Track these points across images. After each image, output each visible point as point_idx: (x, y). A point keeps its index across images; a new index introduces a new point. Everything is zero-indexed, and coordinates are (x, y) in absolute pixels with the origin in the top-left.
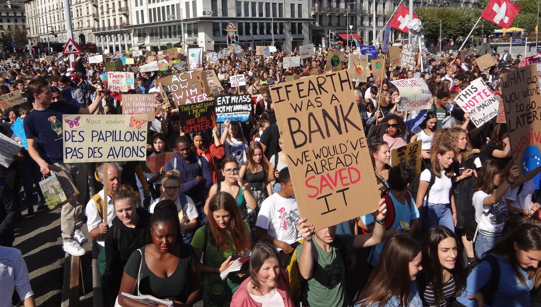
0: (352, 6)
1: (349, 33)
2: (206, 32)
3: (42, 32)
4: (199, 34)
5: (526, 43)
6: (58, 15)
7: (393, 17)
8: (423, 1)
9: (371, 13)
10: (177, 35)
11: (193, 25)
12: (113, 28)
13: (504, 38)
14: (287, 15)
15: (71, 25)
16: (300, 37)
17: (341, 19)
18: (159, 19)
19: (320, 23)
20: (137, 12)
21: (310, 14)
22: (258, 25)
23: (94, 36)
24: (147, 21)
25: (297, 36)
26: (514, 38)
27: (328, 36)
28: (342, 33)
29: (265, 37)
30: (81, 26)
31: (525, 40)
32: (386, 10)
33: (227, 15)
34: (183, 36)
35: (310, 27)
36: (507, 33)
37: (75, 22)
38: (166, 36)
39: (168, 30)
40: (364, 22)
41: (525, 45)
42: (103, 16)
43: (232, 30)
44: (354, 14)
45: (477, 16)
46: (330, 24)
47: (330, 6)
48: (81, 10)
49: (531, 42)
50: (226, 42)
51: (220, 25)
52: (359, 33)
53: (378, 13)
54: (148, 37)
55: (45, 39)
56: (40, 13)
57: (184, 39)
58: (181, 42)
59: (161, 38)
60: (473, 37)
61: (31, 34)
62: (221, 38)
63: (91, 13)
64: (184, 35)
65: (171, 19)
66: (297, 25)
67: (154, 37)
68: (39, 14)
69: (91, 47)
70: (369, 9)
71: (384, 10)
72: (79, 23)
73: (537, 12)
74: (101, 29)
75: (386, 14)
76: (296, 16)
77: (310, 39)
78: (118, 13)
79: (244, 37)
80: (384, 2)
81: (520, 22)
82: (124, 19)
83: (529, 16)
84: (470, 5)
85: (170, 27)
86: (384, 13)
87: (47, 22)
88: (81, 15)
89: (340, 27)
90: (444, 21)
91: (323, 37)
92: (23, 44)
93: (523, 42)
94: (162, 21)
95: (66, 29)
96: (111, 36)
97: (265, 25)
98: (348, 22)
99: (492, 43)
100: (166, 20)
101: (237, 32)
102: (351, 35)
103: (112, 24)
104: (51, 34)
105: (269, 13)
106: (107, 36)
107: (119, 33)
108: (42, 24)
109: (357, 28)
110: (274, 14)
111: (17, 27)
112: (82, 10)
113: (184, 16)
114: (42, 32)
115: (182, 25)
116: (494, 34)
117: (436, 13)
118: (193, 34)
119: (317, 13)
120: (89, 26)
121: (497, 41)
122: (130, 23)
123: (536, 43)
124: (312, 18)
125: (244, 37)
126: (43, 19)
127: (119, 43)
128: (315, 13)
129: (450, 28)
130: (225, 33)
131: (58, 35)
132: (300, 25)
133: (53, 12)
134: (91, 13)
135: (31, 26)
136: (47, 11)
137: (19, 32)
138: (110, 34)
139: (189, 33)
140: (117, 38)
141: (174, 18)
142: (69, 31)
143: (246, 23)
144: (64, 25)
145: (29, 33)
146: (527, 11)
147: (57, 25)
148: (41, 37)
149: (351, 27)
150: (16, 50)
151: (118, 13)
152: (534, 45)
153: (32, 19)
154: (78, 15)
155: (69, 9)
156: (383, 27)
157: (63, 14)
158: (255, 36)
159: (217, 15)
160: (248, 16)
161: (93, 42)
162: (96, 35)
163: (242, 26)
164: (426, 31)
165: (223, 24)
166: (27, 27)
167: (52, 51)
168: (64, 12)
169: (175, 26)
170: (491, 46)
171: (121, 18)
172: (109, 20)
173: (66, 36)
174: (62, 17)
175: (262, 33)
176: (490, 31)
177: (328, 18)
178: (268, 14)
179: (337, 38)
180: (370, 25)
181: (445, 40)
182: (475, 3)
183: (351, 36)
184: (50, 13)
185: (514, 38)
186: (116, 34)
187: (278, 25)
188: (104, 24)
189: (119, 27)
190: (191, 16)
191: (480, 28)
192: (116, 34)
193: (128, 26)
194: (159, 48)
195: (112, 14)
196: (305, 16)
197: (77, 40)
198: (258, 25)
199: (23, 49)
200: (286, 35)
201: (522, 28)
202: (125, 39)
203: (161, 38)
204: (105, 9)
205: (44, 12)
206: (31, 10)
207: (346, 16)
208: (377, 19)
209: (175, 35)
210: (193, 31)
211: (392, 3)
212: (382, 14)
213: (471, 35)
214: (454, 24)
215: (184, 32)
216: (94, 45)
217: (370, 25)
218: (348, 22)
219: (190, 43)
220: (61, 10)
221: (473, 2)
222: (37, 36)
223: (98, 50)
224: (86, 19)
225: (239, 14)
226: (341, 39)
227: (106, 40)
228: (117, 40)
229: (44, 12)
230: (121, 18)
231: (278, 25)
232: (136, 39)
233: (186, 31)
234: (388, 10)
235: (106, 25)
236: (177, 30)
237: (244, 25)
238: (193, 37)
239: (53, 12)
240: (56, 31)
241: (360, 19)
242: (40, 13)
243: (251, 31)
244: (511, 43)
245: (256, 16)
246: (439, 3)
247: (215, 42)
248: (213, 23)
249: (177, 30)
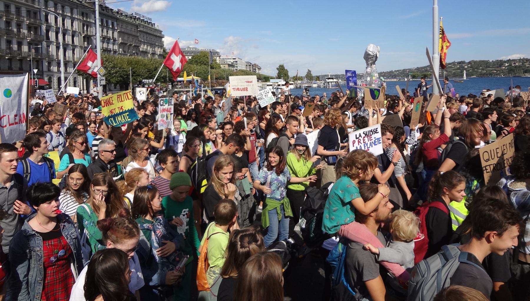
0: (37, 50)
8: (113, 49)
31: (200, 86)
32: (75, 56)
44: (39, 59)
47: (10, 48)
53: (67, 59)
70: (57, 55)
71: (73, 56)
75: (75, 60)
80: (74, 47)
81: (197, 72)
84: (156, 56)
86: (74, 60)
90: (133, 69)
99: (176, 90)
121: (180, 88)
146: (202, 64)
164: (117, 77)
182: (160, 55)
211: (82, 49)
212: (71, 59)
221: (159, 53)
241: (47, 64)
246: (128, 52)
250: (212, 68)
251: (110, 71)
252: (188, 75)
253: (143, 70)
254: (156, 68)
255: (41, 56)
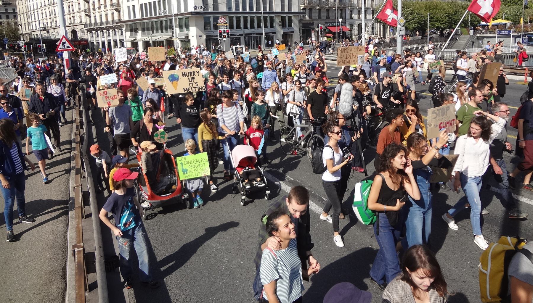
1: (339, 26)
2: (196, 26)
3: (34, 28)
4: (191, 28)
5: (512, 34)
6: (50, 11)
7: (381, 10)
9: (360, 6)
10: (169, 30)
11: (184, 20)
12: (105, 24)
13: (490, 30)
14: (278, 9)
15: (64, 20)
16: (290, 30)
17: (330, 12)
18: (151, 14)
19: (310, 17)
20: (129, 7)
21: (299, 7)
22: (249, 19)
23: (86, 31)
24: (138, 16)
25: (287, 29)
26: (499, 29)
27: (317, 29)
28: (331, 26)
29: (256, 30)
30: (72, 22)
31: (510, 31)
33: (217, 9)
34: (174, 30)
35: (300, 21)
36: (494, 25)
37: (67, 18)
38: (157, 30)
39: (159, 25)
40: (353, 15)
41: (510, 37)
42: (94, 12)
43: (223, 25)
44: (343, 8)
45: (464, 8)
46: (320, 18)
48: (72, 5)
49: (516, 34)
50: (217, 36)
51: (211, 20)
52: (348, 27)
53: (367, 6)
54: (140, 32)
55: (37, 35)
56: (32, 9)
57: (176, 34)
58: (173, 36)
59: (153, 33)
60: (460, 29)
61: (23, 30)
62: (213, 33)
63: (82, 9)
64: (176, 30)
65: (163, 14)
66: (287, 19)
67: (146, 32)
68: (30, 10)
69: (83, 43)
71: (372, 3)
72: (70, 19)
73: (522, 4)
74: (93, 25)
75: (374, 7)
76: (286, 10)
77: (300, 33)
78: (110, 8)
79: (235, 31)
82: (116, 14)
83: (515, 8)
85: (161, 22)
86: (372, 6)
87: (38, 18)
88: (73, 10)
89: (330, 20)
90: (431, 14)
91: (313, 30)
92: (15, 40)
93: (509, 34)
94: (153, 16)
95: (58, 25)
96: (103, 31)
97: (255, 19)
98: (338, 15)
99: (478, 35)
100: (158, 15)
101: (228, 27)
102: (341, 28)
103: (104, 20)
104: (43, 30)
105: (260, 7)
106: (99, 31)
107: (111, 29)
108: (33, 20)
109: (347, 21)
110: (265, 8)
111: (8, 23)
112: (74, 6)
113: (175, 11)
114: (34, 28)
115: (174, 19)
116: (480, 26)
117: (423, 6)
118: (184, 29)
119: (307, 7)
120: (81, 22)
121: (483, 33)
122: (122, 18)
123: (521, 35)
124: (302, 12)
125: (235, 31)
126: (34, 15)
127: (111, 38)
128: (304, 6)
129: (437, 21)
130: (216, 27)
131: (50, 31)
132: (290, 19)
133: (45, 8)
134: (82, 9)
135: (23, 23)
136: (39, 7)
137: (11, 28)
138: (102, 29)
139: (181, 27)
140: (109, 33)
141: (165, 13)
142: (62, 28)
143: (237, 17)
144: (56, 21)
145: (20, 29)
146: (512, 3)
147: (49, 21)
148: (33, 33)
149: (340, 20)
150: (8, 46)
151: (110, 8)
152: (519, 37)
153: (24, 15)
154: (69, 11)
155: (62, 5)
156: (371, 20)
157: (55, 10)
158: (246, 30)
159: (208, 9)
160: (239, 10)
161: (85, 37)
162: (88, 30)
163: (233, 20)
165: (214, 18)
166: (19, 23)
167: (45, 47)
168: (56, 8)
169: (166, 21)
170: (478, 38)
171: (113, 14)
172: (101, 15)
173: (58, 32)
174: (54, 13)
175: (252, 27)
176: (476, 23)
177: (318, 12)
178: (258, 8)
179: (327, 31)
180: (359, 18)
181: (432, 32)
183: (341, 30)
184: (41, 9)
185: (499, 29)
186: (108, 29)
187: (268, 18)
188: (96, 19)
189: (111, 23)
190: (183, 11)
191: (467, 21)
192: (108, 29)
193: (120, 21)
194: (151, 42)
195: (104, 9)
196: (295, 9)
197: (70, 36)
198: (249, 19)
199: (15, 45)
200: (276, 29)
201: (508, 19)
202: (117, 34)
203: (153, 33)
204: (97, 6)
205: (35, 8)
206: (22, 6)
207: (335, 10)
208: (365, 11)
209: (167, 29)
210: (184, 26)
212: (370, 7)
213: (458, 27)
214: (442, 16)
215: (176, 27)
216: (87, 41)
217: (359, 18)
218: (338, 15)
219: (181, 37)
220: (53, 6)
222: (29, 32)
223: (90, 44)
224: (78, 15)
225: (230, 8)
226: (330, 32)
227: (98, 36)
228: (109, 35)
229: (35, 8)
230: (113, 14)
231: (268, 18)
232: (128, 34)
233: (178, 26)
234: (377, 3)
235: (98, 21)
236: (169, 24)
237: (234, 19)
238: (184, 32)
239: (45, 8)
240: (48, 27)
241: (349, 12)
242: (32, 9)
243: (242, 25)
244: (497, 35)
245: (246, 10)
247: (207, 36)
248: (204, 17)
249: (169, 24)
250: (526, 7)
251: (407, 17)
252: (494, 19)
253: (442, 15)
254: (457, 12)
255: (345, 5)
